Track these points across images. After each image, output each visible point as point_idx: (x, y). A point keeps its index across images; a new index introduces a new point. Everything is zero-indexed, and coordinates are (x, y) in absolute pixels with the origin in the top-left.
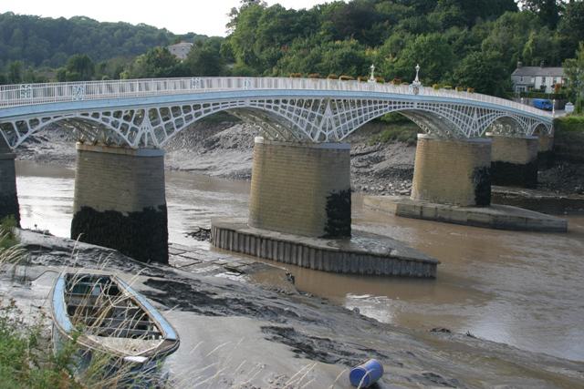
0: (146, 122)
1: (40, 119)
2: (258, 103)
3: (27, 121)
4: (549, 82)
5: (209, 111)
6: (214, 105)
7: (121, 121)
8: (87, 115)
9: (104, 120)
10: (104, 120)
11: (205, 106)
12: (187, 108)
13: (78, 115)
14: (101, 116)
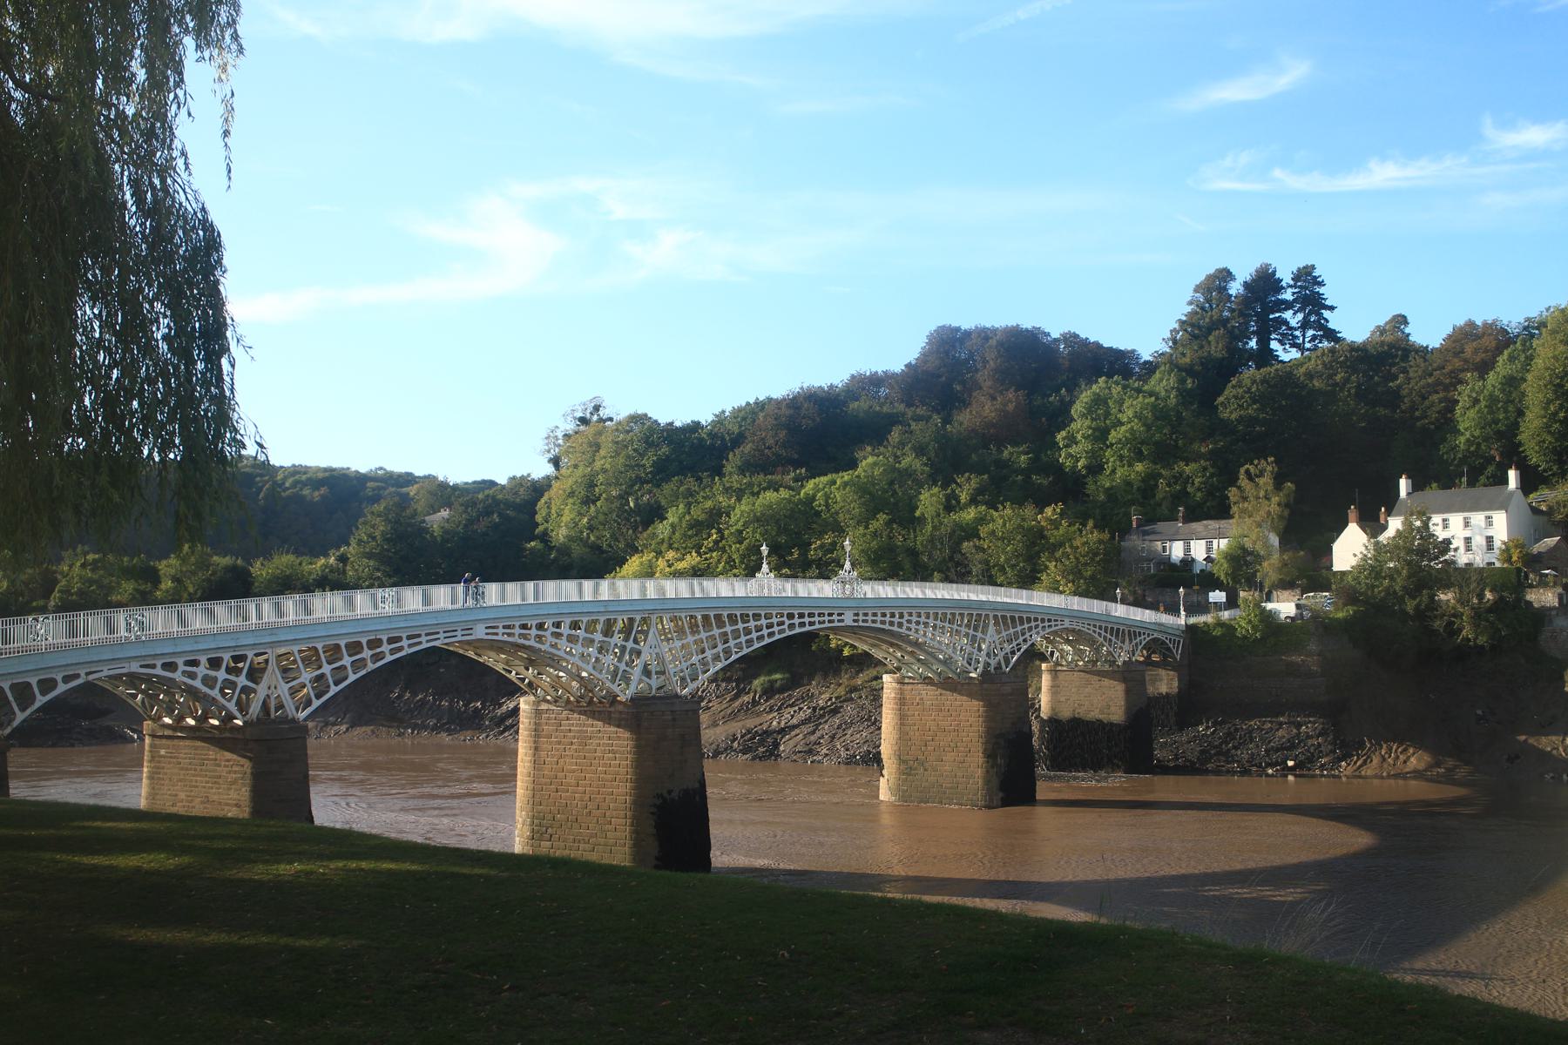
0: (272, 676)
1: (59, 678)
2: (501, 630)
3: (33, 681)
6: (409, 638)
7: (221, 675)
8: (154, 666)
12: (355, 647)
13: (135, 667)
14: (182, 668)
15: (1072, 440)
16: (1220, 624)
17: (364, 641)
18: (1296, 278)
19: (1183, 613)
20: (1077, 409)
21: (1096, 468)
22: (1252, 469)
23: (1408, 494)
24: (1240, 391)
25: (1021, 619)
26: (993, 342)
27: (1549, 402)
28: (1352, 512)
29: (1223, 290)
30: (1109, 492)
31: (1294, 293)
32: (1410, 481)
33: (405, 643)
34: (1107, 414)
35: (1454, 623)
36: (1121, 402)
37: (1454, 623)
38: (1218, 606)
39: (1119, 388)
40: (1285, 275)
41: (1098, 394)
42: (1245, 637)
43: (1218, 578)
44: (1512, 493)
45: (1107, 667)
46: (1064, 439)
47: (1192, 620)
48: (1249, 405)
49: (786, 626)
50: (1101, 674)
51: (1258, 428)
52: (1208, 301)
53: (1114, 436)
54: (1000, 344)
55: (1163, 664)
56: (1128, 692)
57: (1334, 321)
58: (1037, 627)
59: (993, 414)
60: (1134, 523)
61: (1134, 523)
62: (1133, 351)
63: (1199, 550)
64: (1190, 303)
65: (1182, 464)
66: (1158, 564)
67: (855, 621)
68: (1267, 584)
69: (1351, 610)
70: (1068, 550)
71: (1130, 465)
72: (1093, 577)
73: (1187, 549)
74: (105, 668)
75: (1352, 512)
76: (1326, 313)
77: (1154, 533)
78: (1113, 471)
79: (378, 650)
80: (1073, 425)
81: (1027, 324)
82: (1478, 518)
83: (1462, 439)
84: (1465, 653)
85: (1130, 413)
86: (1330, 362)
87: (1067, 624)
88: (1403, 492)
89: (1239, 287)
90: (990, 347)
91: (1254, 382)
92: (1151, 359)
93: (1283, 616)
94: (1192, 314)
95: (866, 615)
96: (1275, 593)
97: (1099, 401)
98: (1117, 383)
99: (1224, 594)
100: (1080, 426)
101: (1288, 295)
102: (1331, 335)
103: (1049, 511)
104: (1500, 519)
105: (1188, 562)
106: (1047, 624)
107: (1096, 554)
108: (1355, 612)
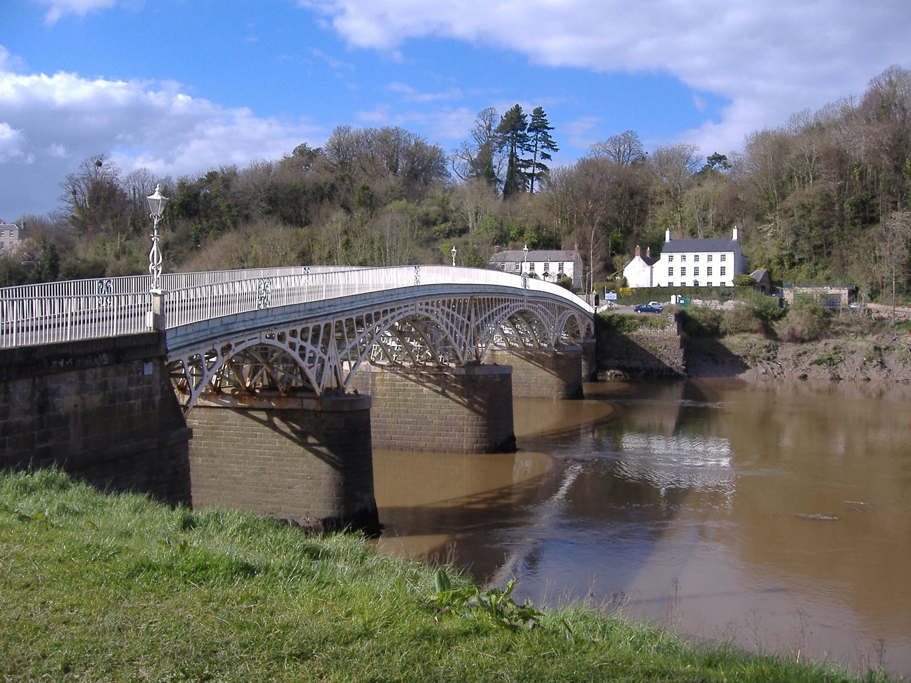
8: (271, 337)
13: (263, 338)
14: (289, 339)
40: (528, 110)
76: (549, 132)
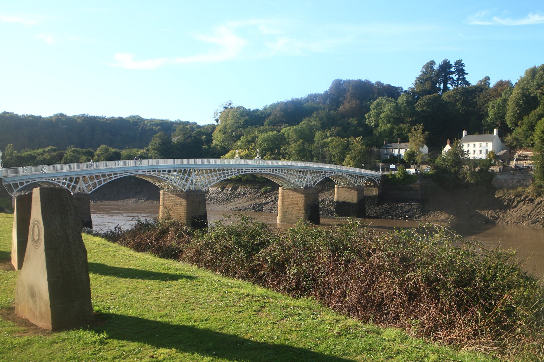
1: (25, 182)
2: (147, 172)
3: (18, 183)
4: (402, 152)
5: (117, 176)
6: (119, 174)
8: (49, 180)
9: (57, 182)
10: (57, 182)
11: (114, 174)
12: (104, 176)
14: (56, 180)
15: (370, 117)
16: (392, 175)
17: (107, 174)
18: (456, 64)
19: (381, 171)
20: (372, 107)
21: (377, 125)
22: (416, 127)
23: (465, 136)
24: (422, 102)
25: (316, 172)
26: (351, 85)
27: (515, 107)
28: (448, 141)
29: (432, 67)
30: (380, 133)
31: (455, 69)
32: (466, 132)
33: (118, 175)
34: (381, 108)
35: (465, 176)
36: (385, 105)
37: (465, 176)
38: (393, 169)
39: (385, 100)
40: (453, 63)
41: (379, 102)
42: (398, 179)
43: (405, 161)
44: (495, 136)
45: (352, 187)
46: (367, 116)
47: (385, 173)
48: (424, 107)
49: (237, 172)
50: (350, 188)
51: (426, 114)
52: (427, 71)
53: (382, 115)
54: (353, 85)
55: (374, 186)
56: (358, 194)
57: (467, 78)
58: (325, 174)
59: (348, 108)
60: (385, 143)
61: (385, 143)
62: (401, 87)
63: (402, 152)
64: (421, 72)
65: (402, 125)
66: (391, 156)
67: (260, 171)
68: (418, 162)
69: (434, 171)
70: (353, 151)
71: (386, 125)
72: (359, 159)
73: (399, 152)
74: (36, 180)
75: (448, 141)
76: (466, 76)
77: (391, 146)
78: (381, 127)
79: (111, 177)
80: (370, 112)
81: (363, 79)
82: (484, 144)
83: (489, 118)
84: (468, 185)
85: (387, 109)
86: (456, 92)
87: (336, 173)
88: (464, 136)
89: (437, 67)
90: (350, 86)
91: (426, 99)
92: (408, 90)
93: (411, 173)
94: (421, 75)
95: (242, 169)
96: (421, 166)
97: (378, 104)
98: (385, 99)
99: (394, 166)
100: (373, 112)
101: (453, 69)
102: (467, 83)
103: (357, 139)
104: (490, 144)
105: (399, 155)
106: (329, 173)
107: (360, 153)
108: (435, 172)
